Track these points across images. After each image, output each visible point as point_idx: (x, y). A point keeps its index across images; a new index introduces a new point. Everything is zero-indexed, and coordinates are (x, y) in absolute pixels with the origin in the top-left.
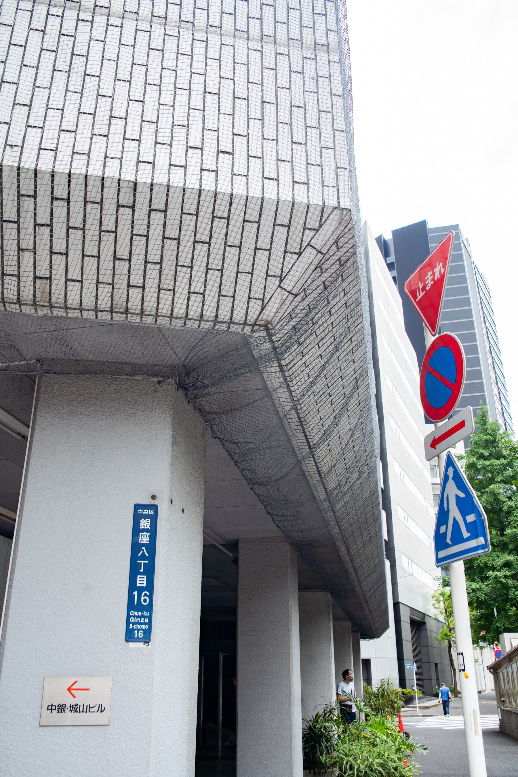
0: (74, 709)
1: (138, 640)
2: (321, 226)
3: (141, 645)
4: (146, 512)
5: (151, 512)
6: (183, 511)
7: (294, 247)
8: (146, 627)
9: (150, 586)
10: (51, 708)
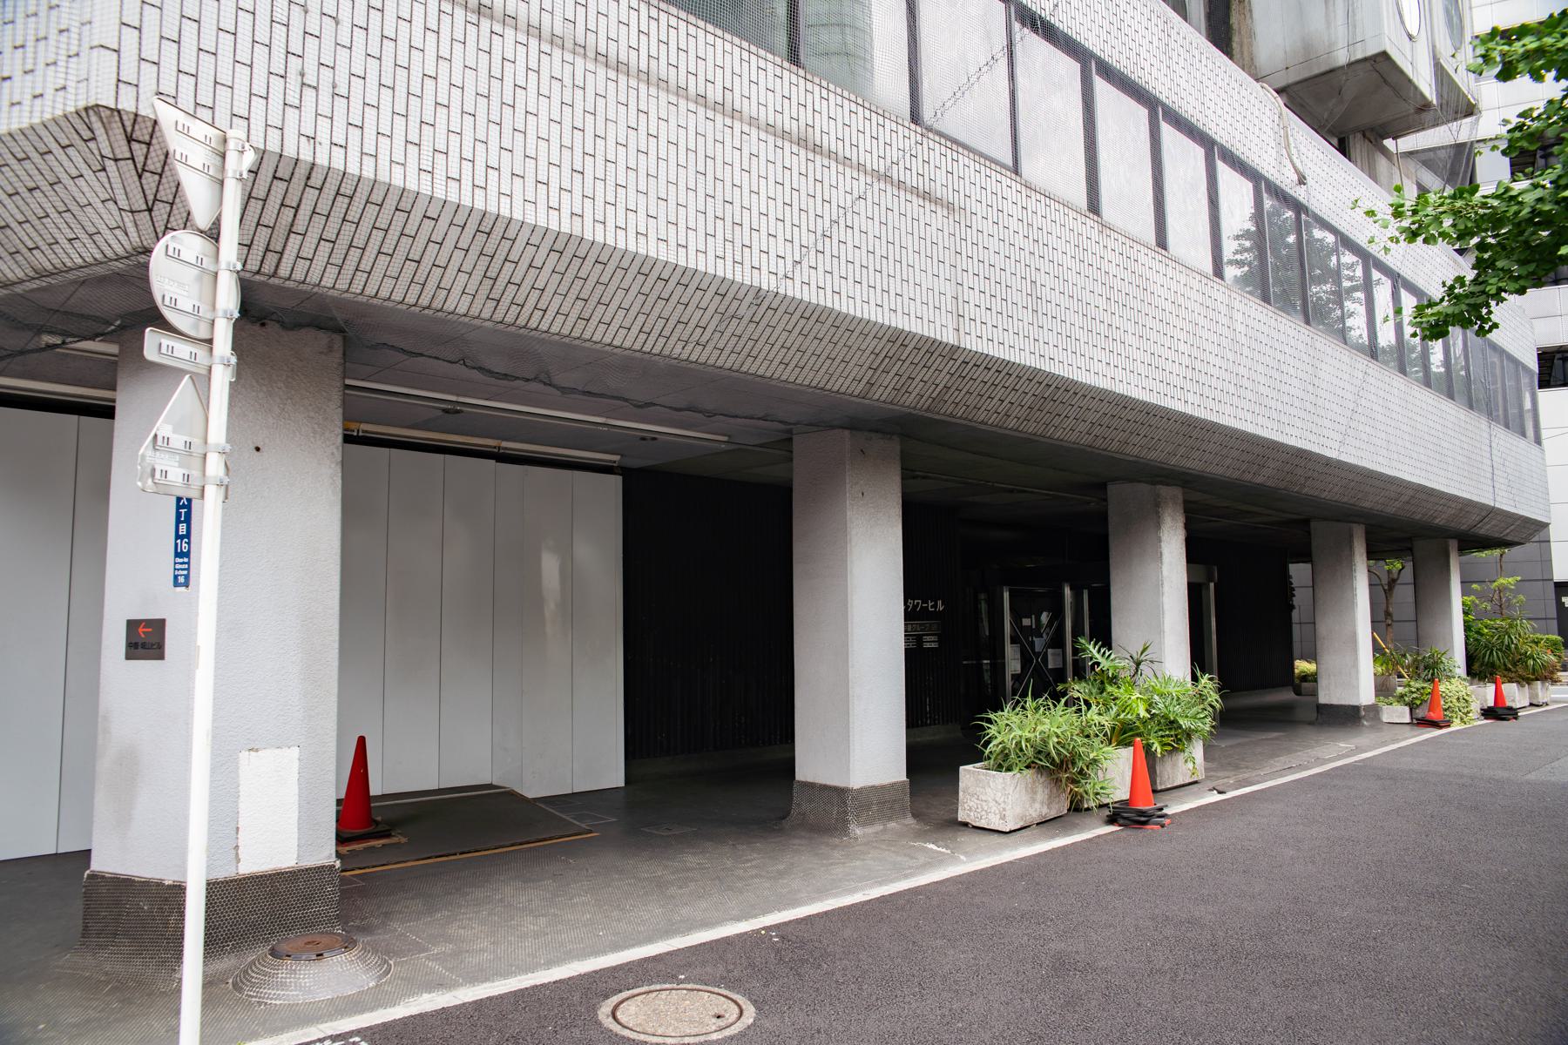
3: (183, 589)
6: (258, 449)
8: (185, 572)
9: (188, 535)
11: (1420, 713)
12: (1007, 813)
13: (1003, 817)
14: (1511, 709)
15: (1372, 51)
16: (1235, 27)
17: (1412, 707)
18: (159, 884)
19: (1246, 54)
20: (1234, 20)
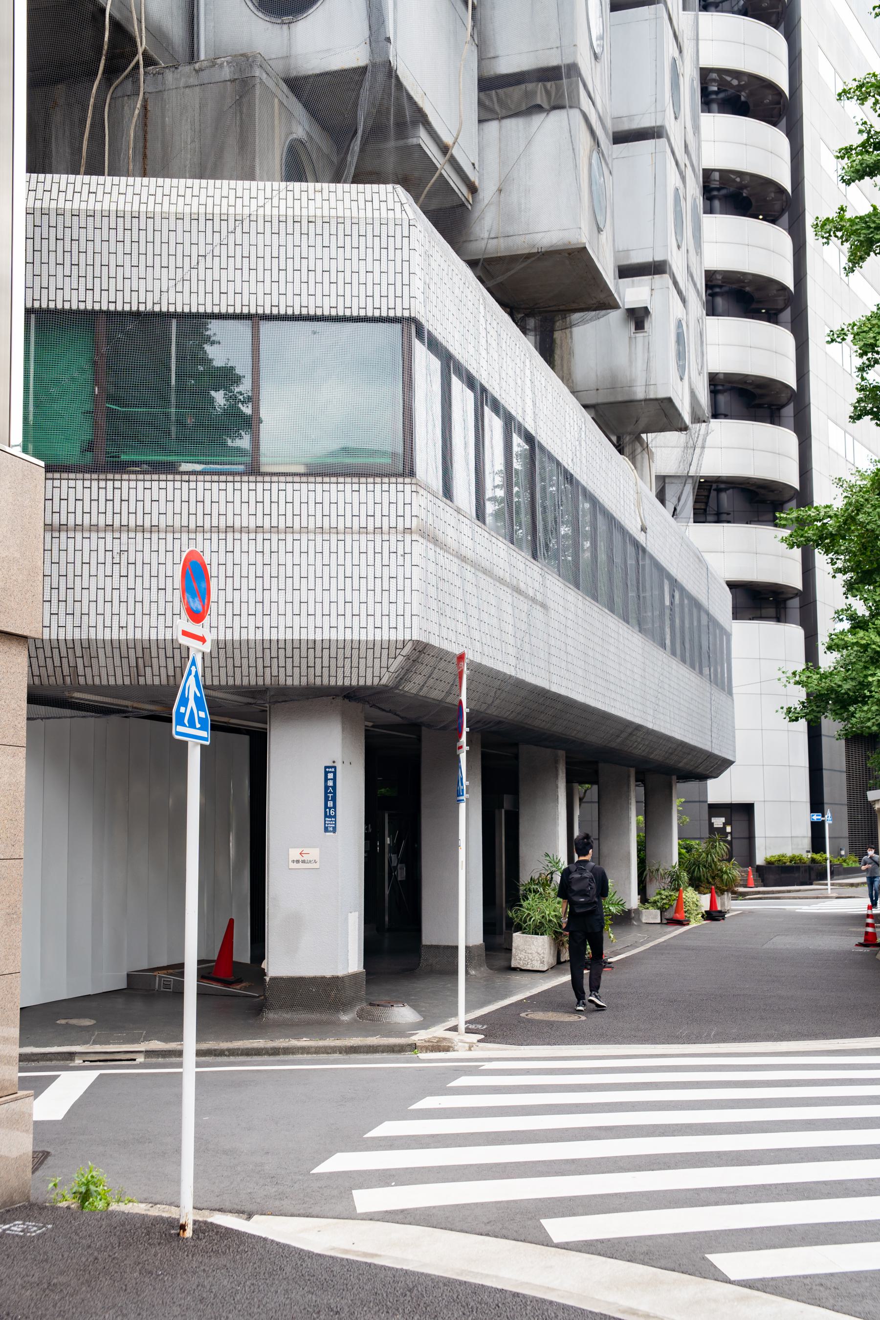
0: (303, 862)
4: (330, 770)
5: (333, 770)
7: (392, 655)
9: (335, 807)
10: (293, 861)
11: (669, 915)
12: (545, 960)
13: (542, 962)
14: (720, 912)
15: (661, 394)
16: (558, 341)
17: (662, 910)
18: (323, 978)
19: (565, 368)
20: (557, 335)
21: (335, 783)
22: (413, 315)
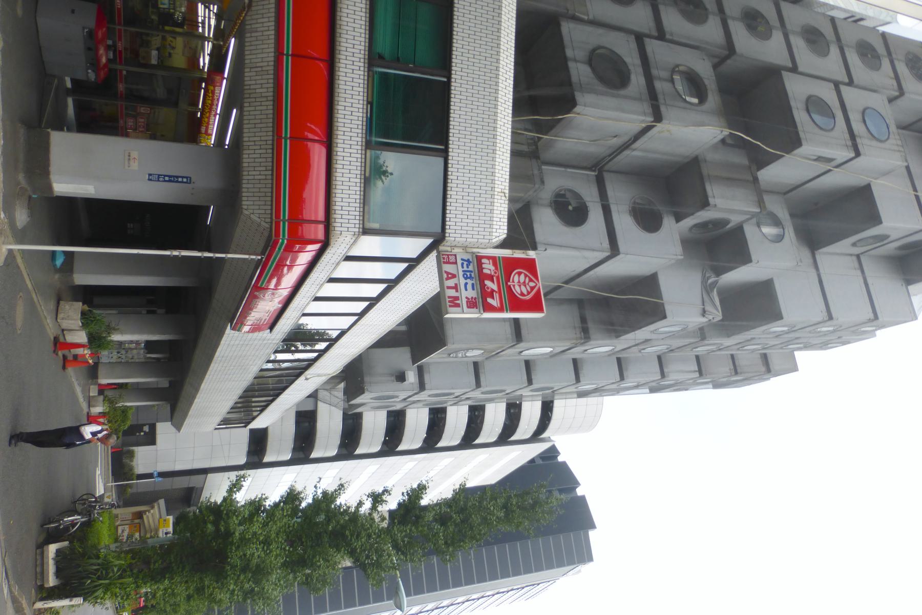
0: (129, 159)
1: (149, 177)
2: (266, 222)
3: (147, 178)
4: (189, 180)
5: (189, 182)
6: (192, 194)
10: (129, 153)
21: (180, 182)
22: (446, 238)
